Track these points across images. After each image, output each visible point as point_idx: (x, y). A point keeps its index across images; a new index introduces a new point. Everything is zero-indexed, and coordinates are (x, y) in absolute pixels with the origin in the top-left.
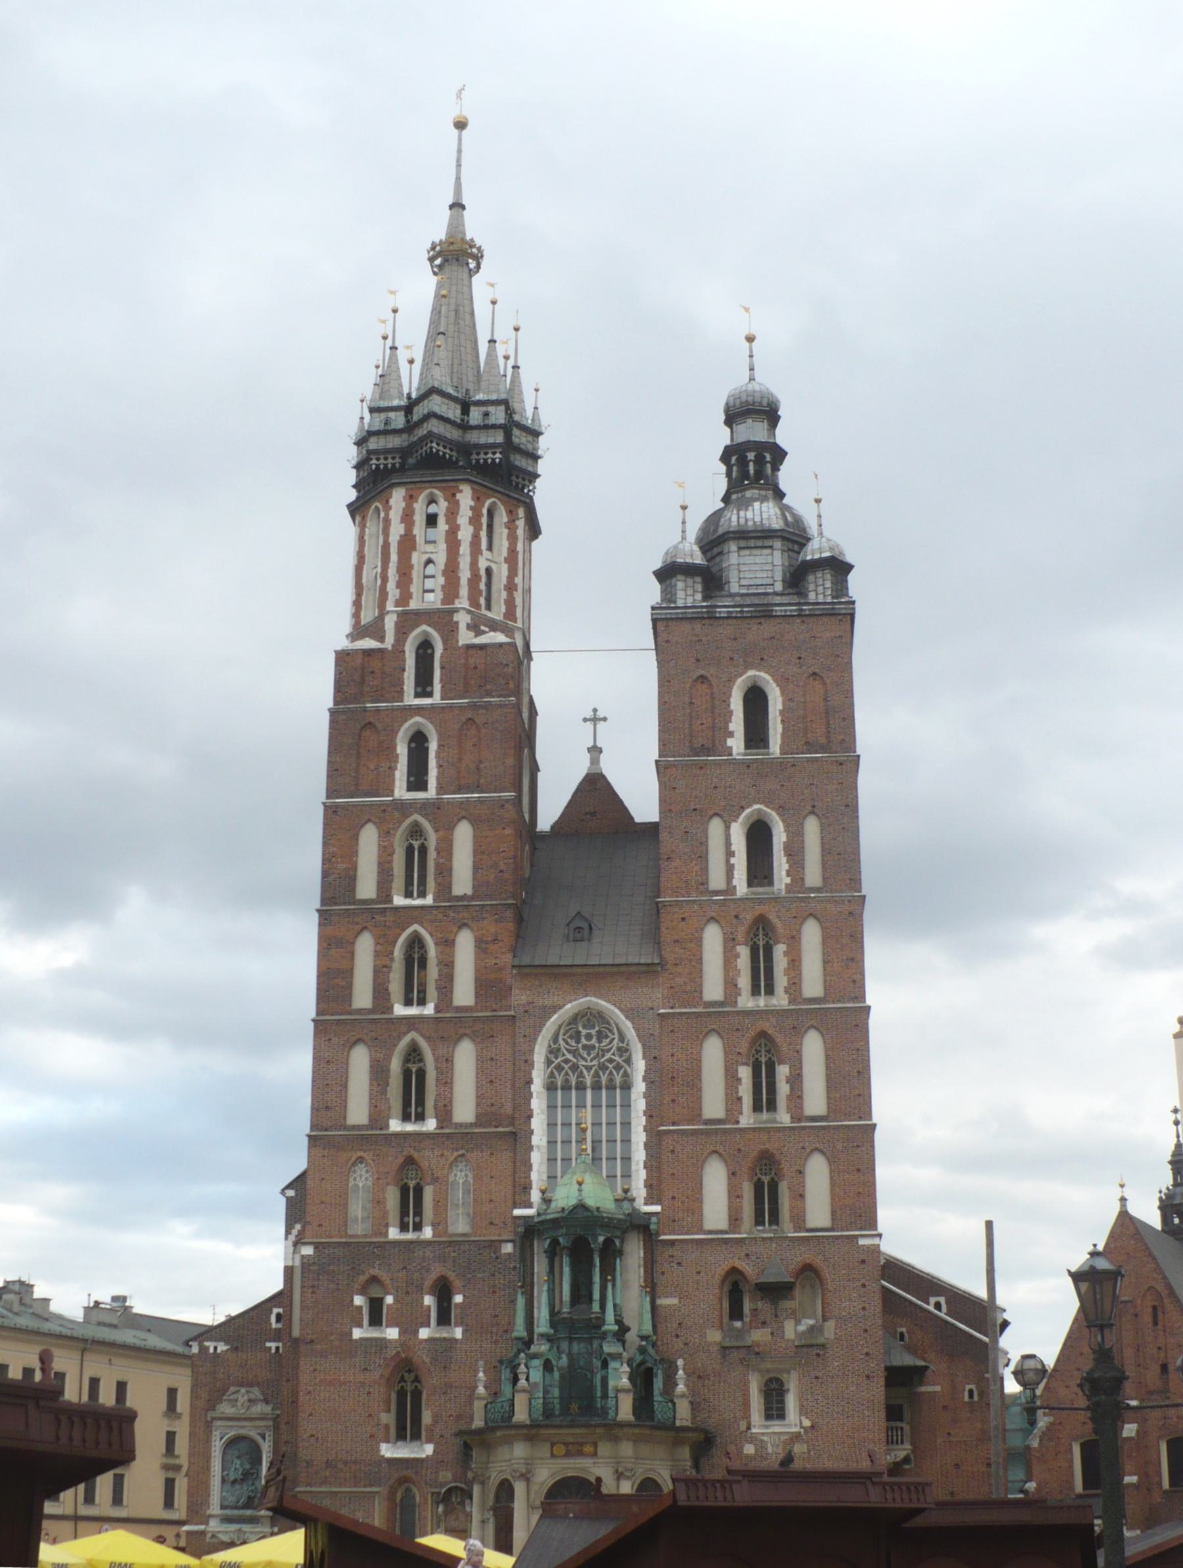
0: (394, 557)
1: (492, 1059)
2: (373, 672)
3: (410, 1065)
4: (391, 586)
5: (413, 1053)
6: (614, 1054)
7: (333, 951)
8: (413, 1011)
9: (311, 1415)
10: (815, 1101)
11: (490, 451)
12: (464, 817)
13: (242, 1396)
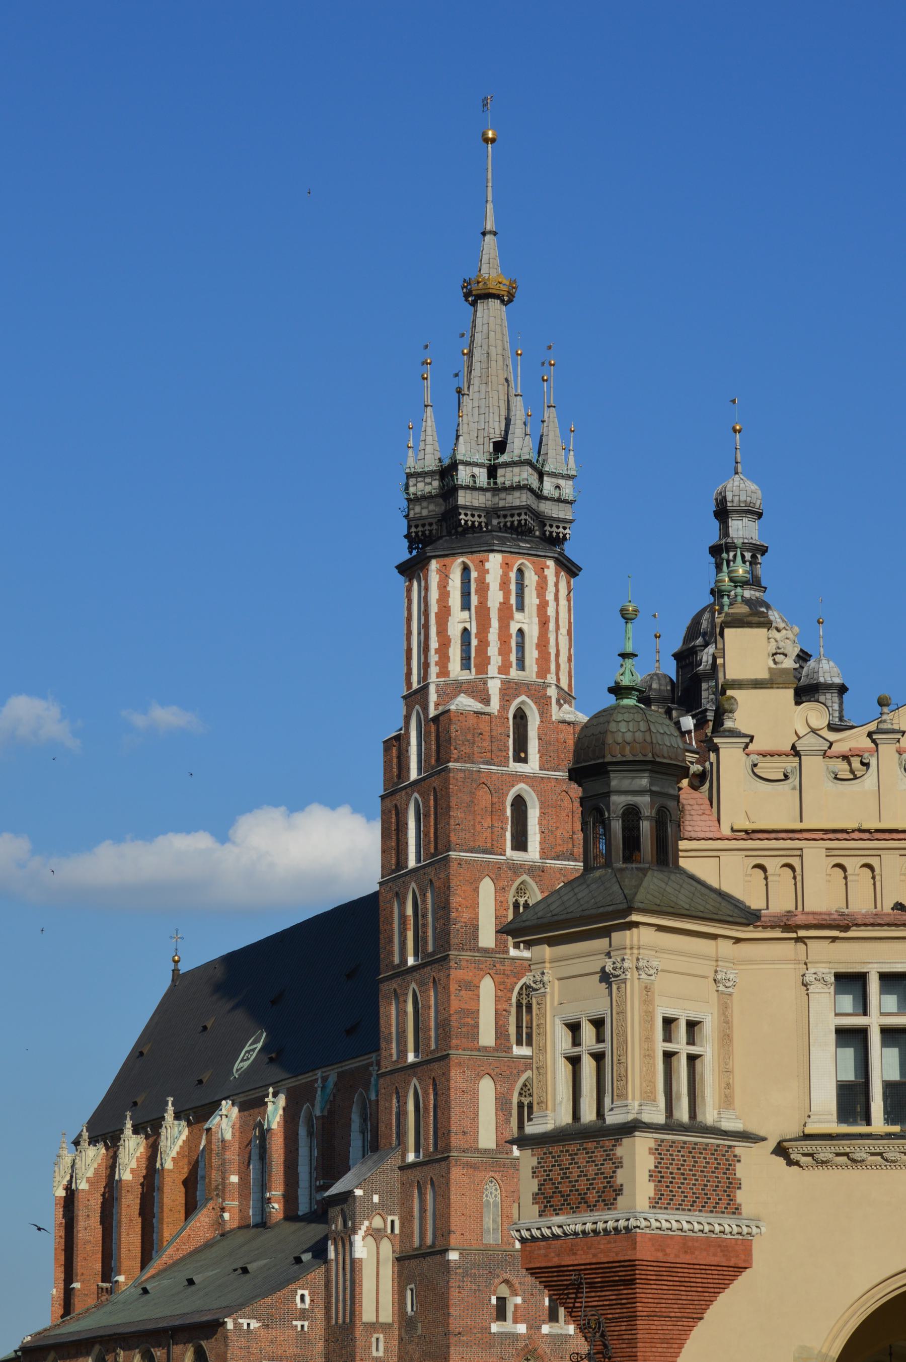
2: (481, 734)
3: (523, 1099)
4: (493, 650)
7: (463, 993)
8: (525, 1051)
11: (561, 525)
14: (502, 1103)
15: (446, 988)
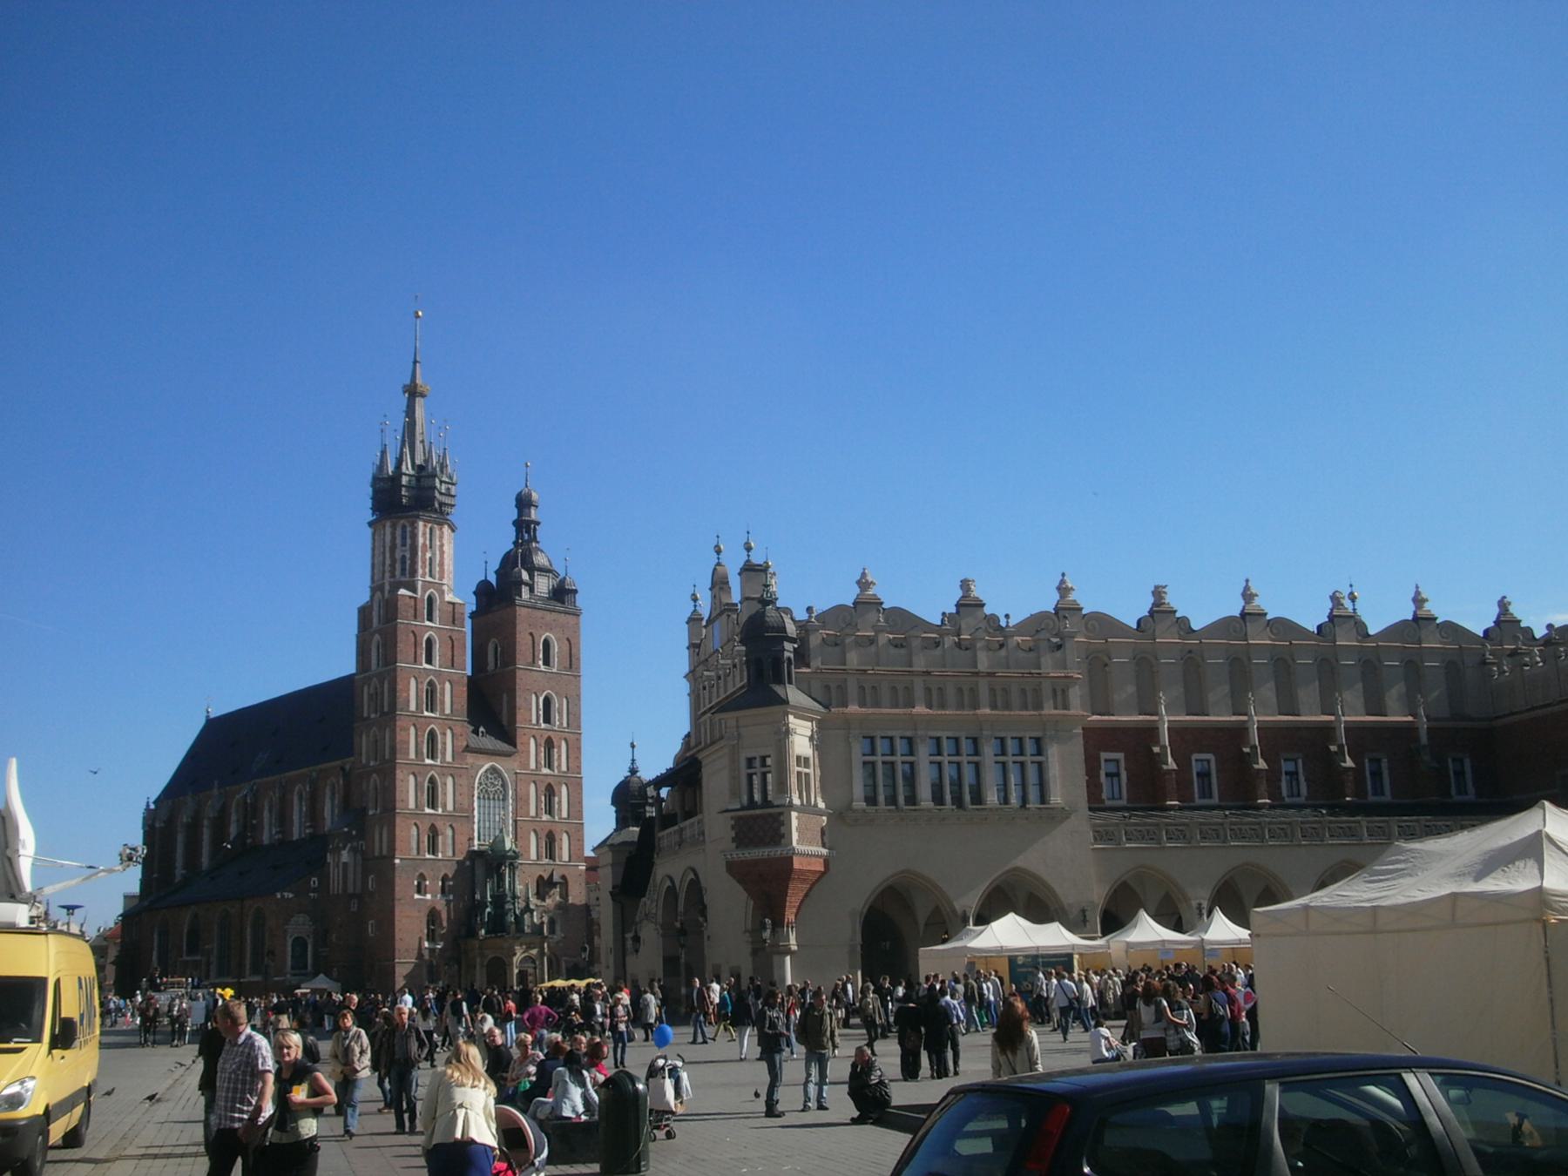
5: (432, 781)
7: (402, 733)
12: (449, 681)
13: (301, 918)
15: (393, 732)
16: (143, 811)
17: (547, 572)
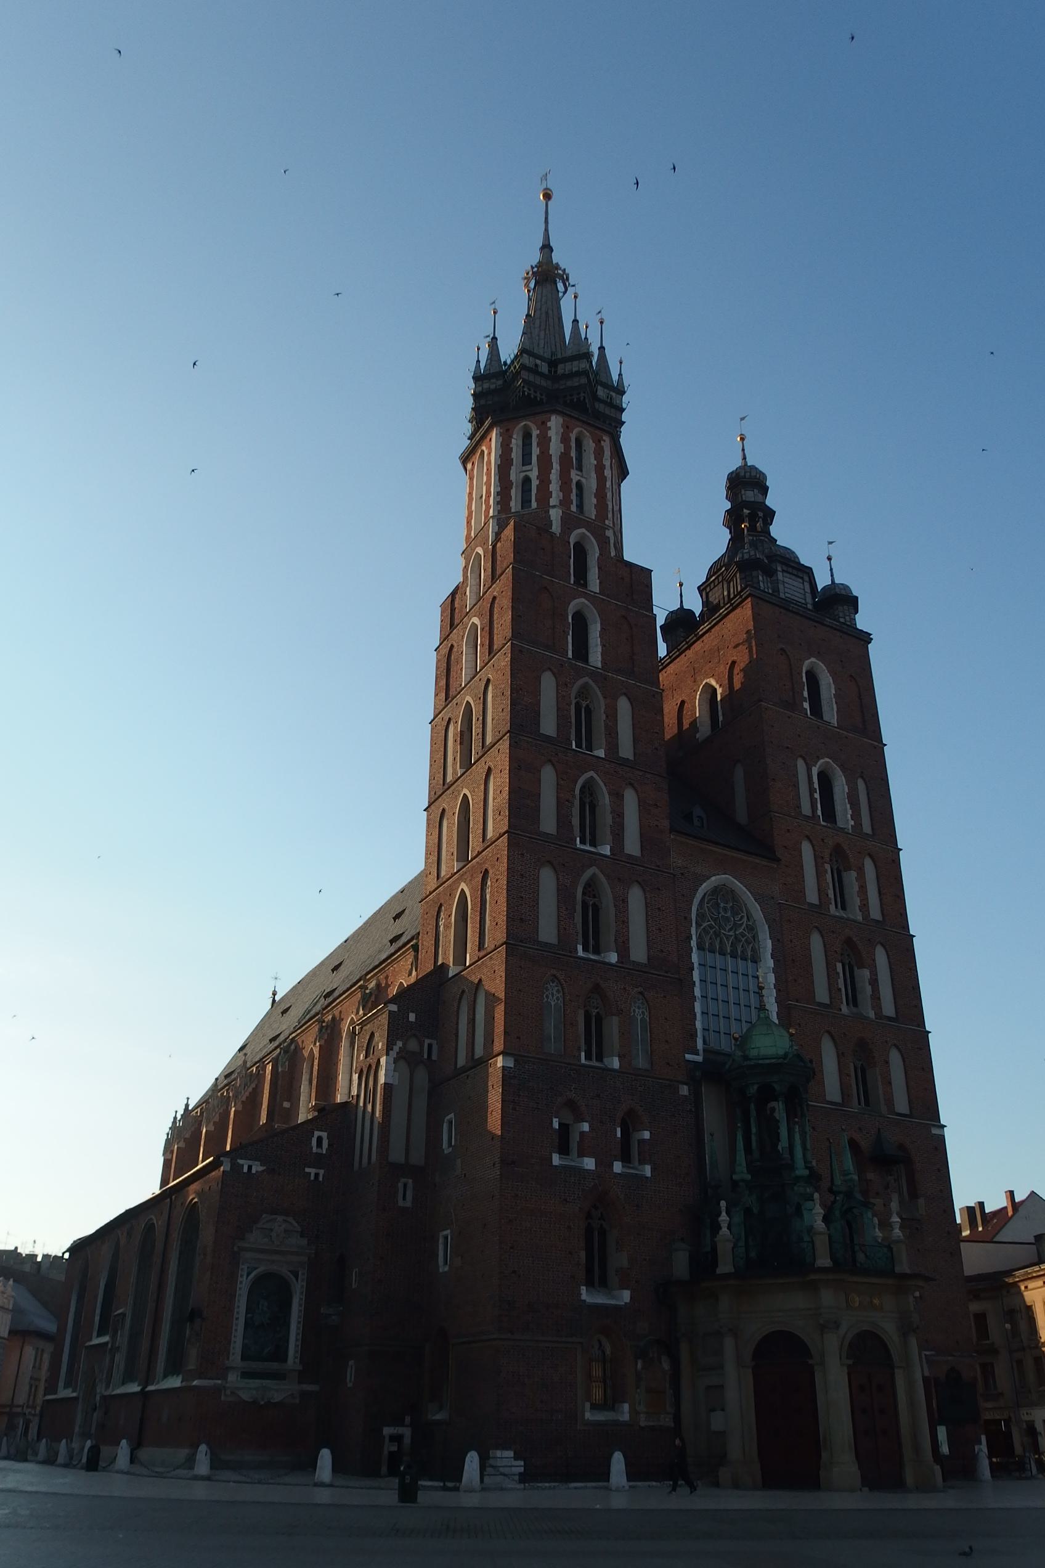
0: (556, 466)
1: (659, 909)
4: (554, 487)
5: (591, 887)
6: (744, 930)
8: (587, 848)
9: (512, 1248)
10: (888, 1008)
12: (625, 694)
14: (564, 895)
16: (167, 1130)
17: (799, 570)
